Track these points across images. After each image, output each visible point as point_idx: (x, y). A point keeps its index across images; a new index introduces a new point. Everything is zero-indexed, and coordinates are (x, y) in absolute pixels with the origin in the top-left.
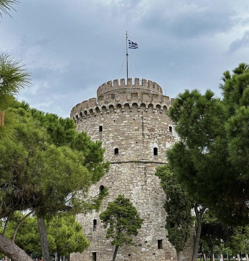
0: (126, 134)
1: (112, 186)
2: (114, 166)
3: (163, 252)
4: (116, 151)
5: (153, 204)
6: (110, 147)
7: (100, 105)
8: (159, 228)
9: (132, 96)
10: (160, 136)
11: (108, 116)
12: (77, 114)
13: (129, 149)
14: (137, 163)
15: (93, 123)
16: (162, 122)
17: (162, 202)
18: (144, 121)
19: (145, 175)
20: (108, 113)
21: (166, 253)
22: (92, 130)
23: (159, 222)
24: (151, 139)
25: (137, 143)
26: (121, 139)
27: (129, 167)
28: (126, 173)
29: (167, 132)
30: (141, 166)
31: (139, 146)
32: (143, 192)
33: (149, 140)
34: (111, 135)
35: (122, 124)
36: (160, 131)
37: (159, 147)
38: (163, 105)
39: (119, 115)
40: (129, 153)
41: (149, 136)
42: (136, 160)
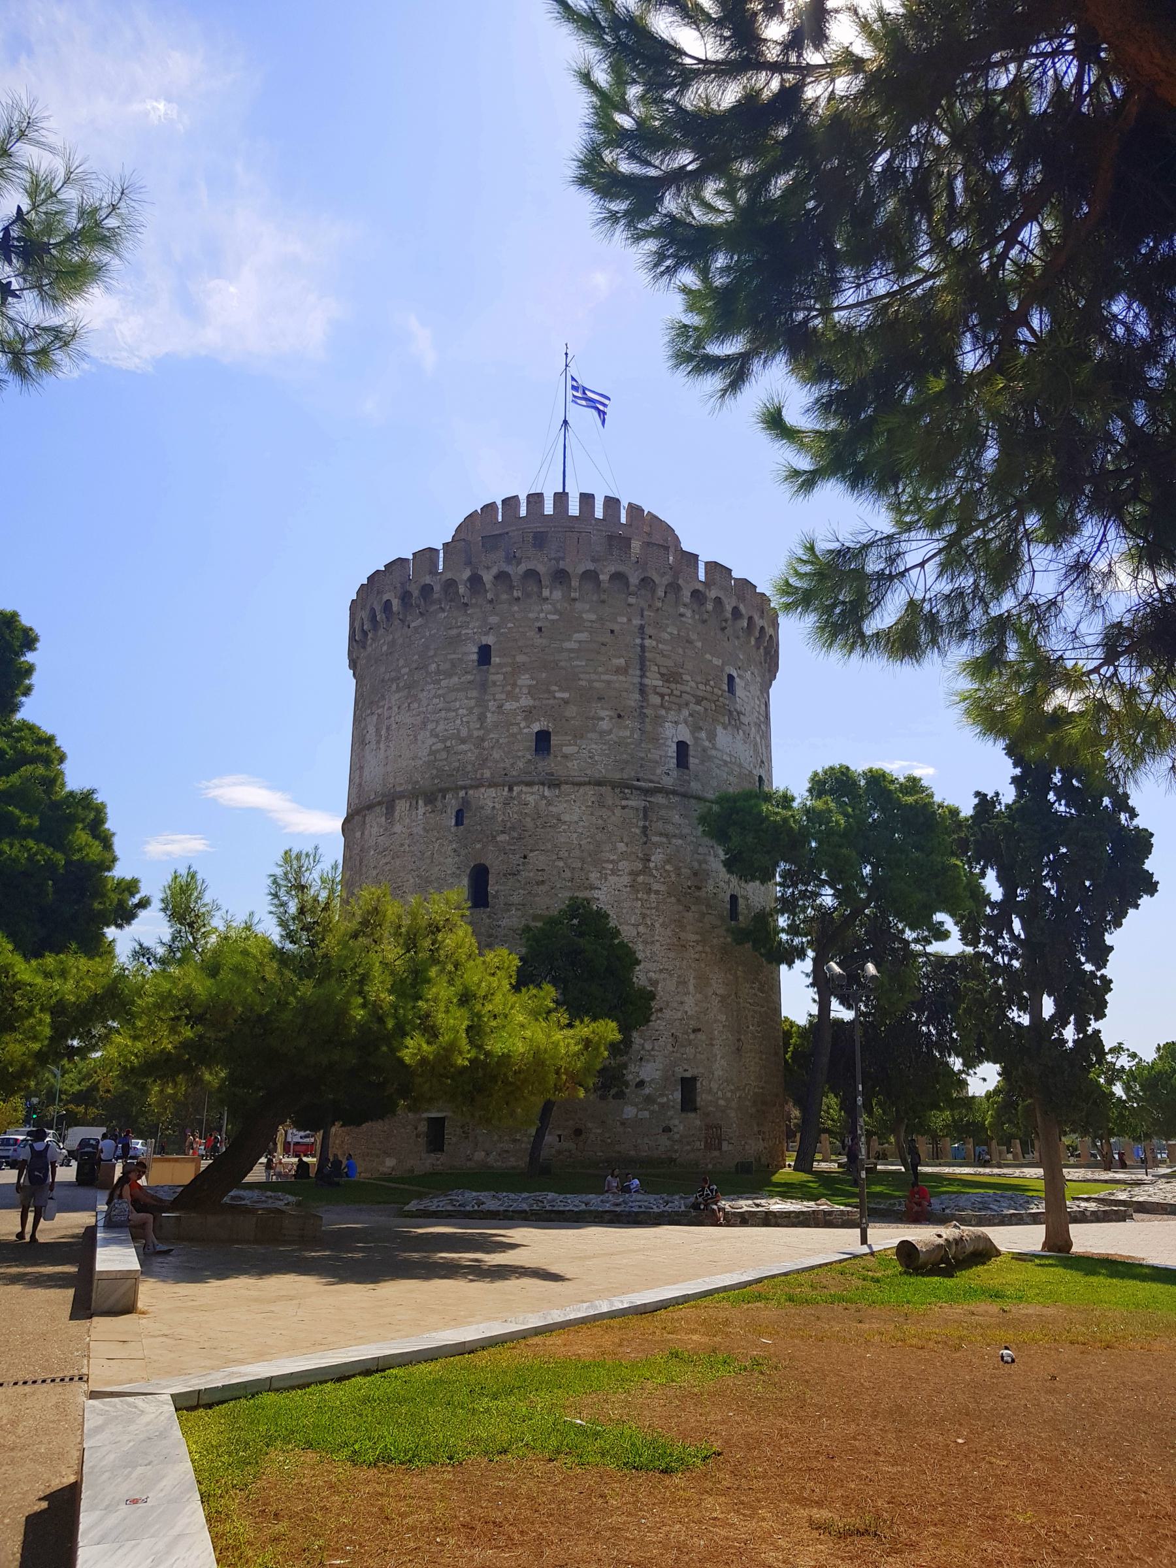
0: (581, 683)
1: (521, 868)
2: (532, 793)
3: (698, 1122)
4: (543, 740)
5: (669, 944)
6: (518, 724)
7: (488, 568)
8: (687, 1033)
9: (610, 545)
10: (698, 703)
11: (516, 608)
12: (386, 597)
13: (589, 735)
14: (618, 790)
15: (454, 632)
17: (698, 937)
18: (647, 642)
19: (646, 836)
20: (518, 599)
21: (709, 1127)
22: (450, 657)
23: (686, 1012)
24: (670, 709)
25: (619, 716)
26: (563, 699)
27: (590, 804)
28: (577, 822)
29: (720, 693)
30: (630, 803)
31: (626, 727)
32: (637, 899)
33: (663, 712)
34: (525, 680)
35: (567, 645)
36: (700, 686)
37: (696, 739)
38: (713, 594)
39: (556, 612)
40: (590, 752)
41: (662, 696)
42: (617, 776)
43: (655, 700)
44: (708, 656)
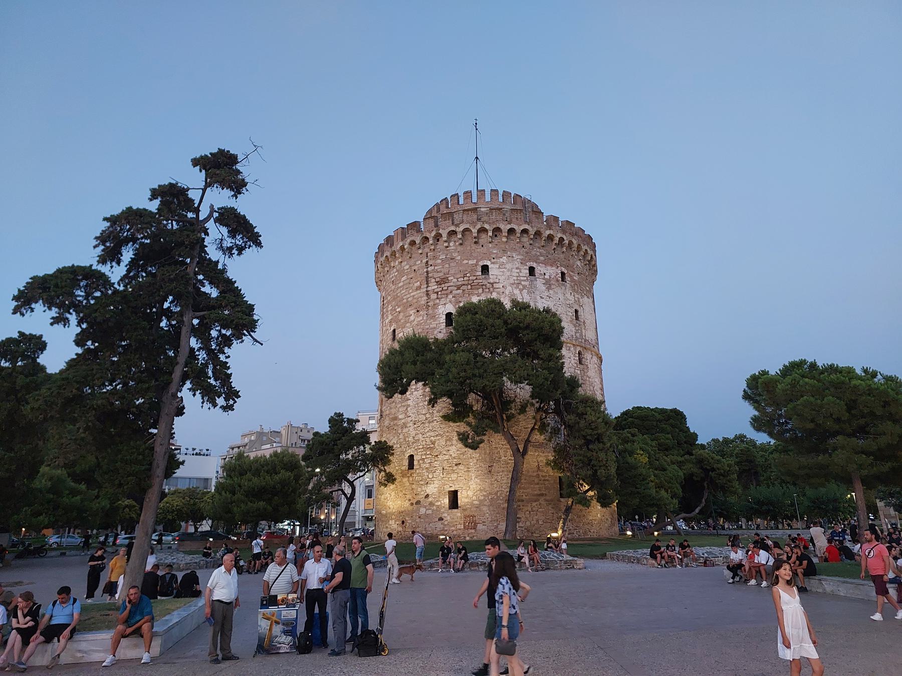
10: (458, 289)
16: (463, 260)
23: (451, 455)
43: (434, 296)
44: (465, 262)
